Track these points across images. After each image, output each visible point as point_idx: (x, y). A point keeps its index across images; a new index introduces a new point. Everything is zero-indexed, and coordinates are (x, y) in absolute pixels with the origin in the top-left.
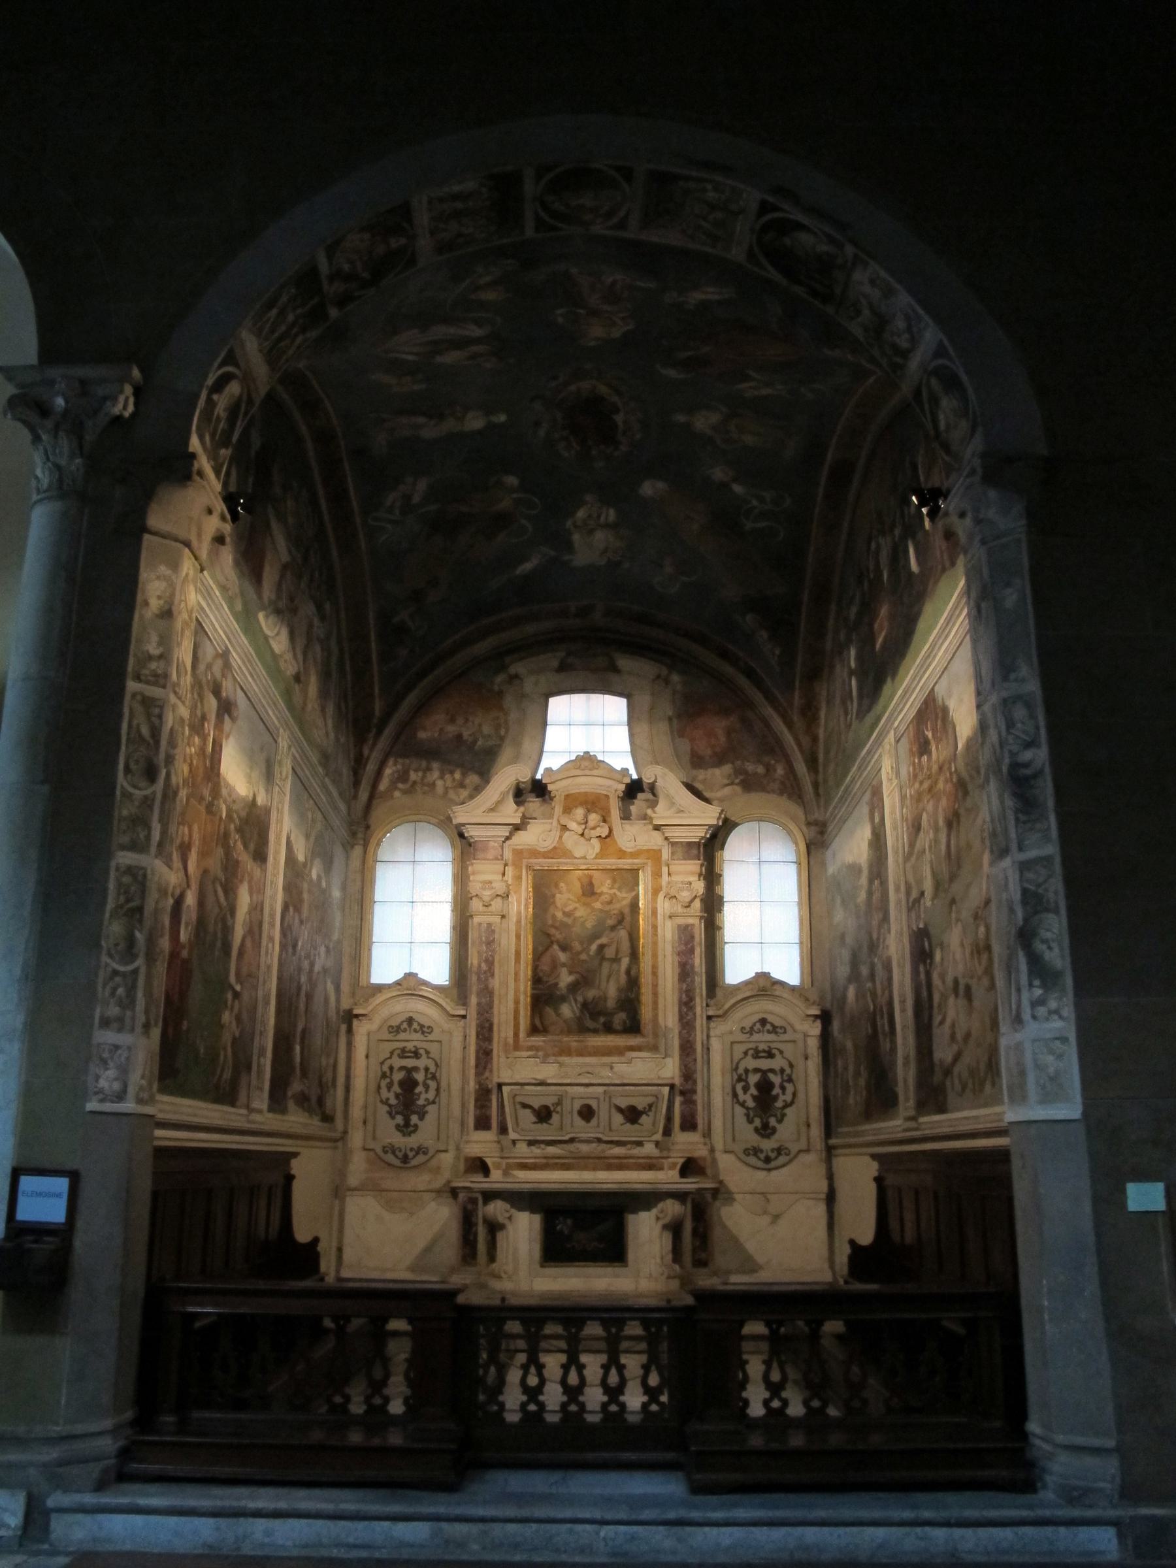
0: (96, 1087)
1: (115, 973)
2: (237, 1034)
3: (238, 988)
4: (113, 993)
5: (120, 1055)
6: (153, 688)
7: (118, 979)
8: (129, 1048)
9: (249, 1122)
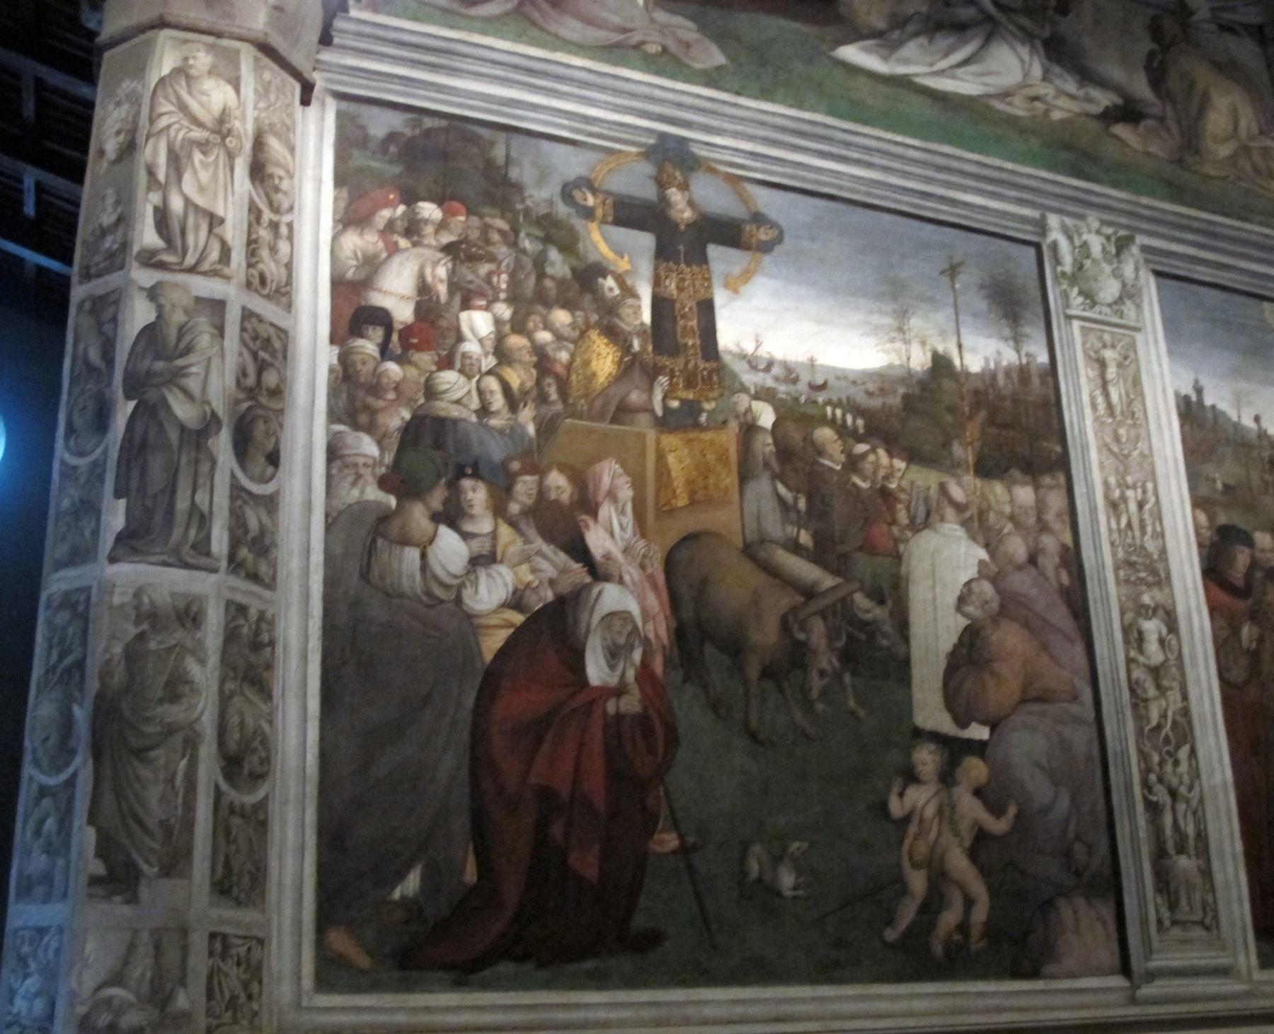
0: (10, 1013)
1: (43, 791)
2: (999, 826)
3: (979, 732)
4: (38, 833)
5: (47, 947)
6: (108, 278)
7: (46, 803)
8: (61, 930)
9: (1133, 1000)
